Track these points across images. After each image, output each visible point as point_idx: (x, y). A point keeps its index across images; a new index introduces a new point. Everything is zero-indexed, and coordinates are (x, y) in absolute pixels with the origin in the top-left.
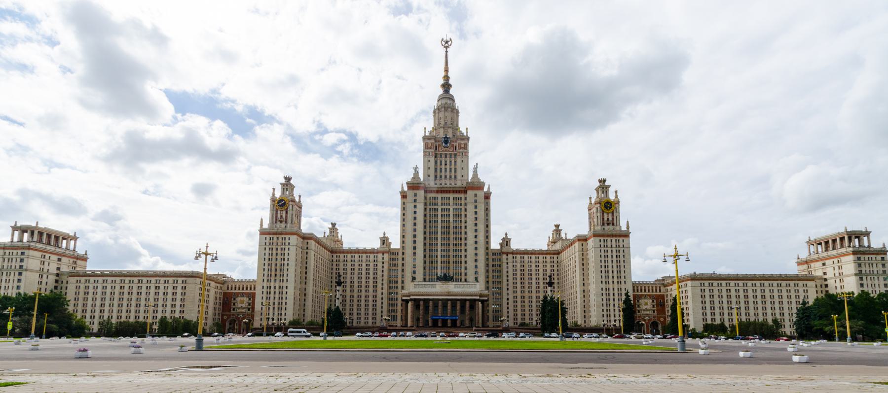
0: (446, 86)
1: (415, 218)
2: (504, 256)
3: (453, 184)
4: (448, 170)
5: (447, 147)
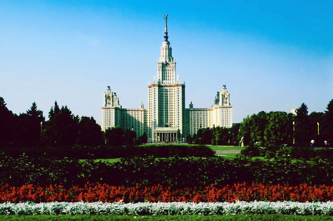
0: (166, 37)
2: (190, 112)
3: (169, 83)
4: (167, 76)
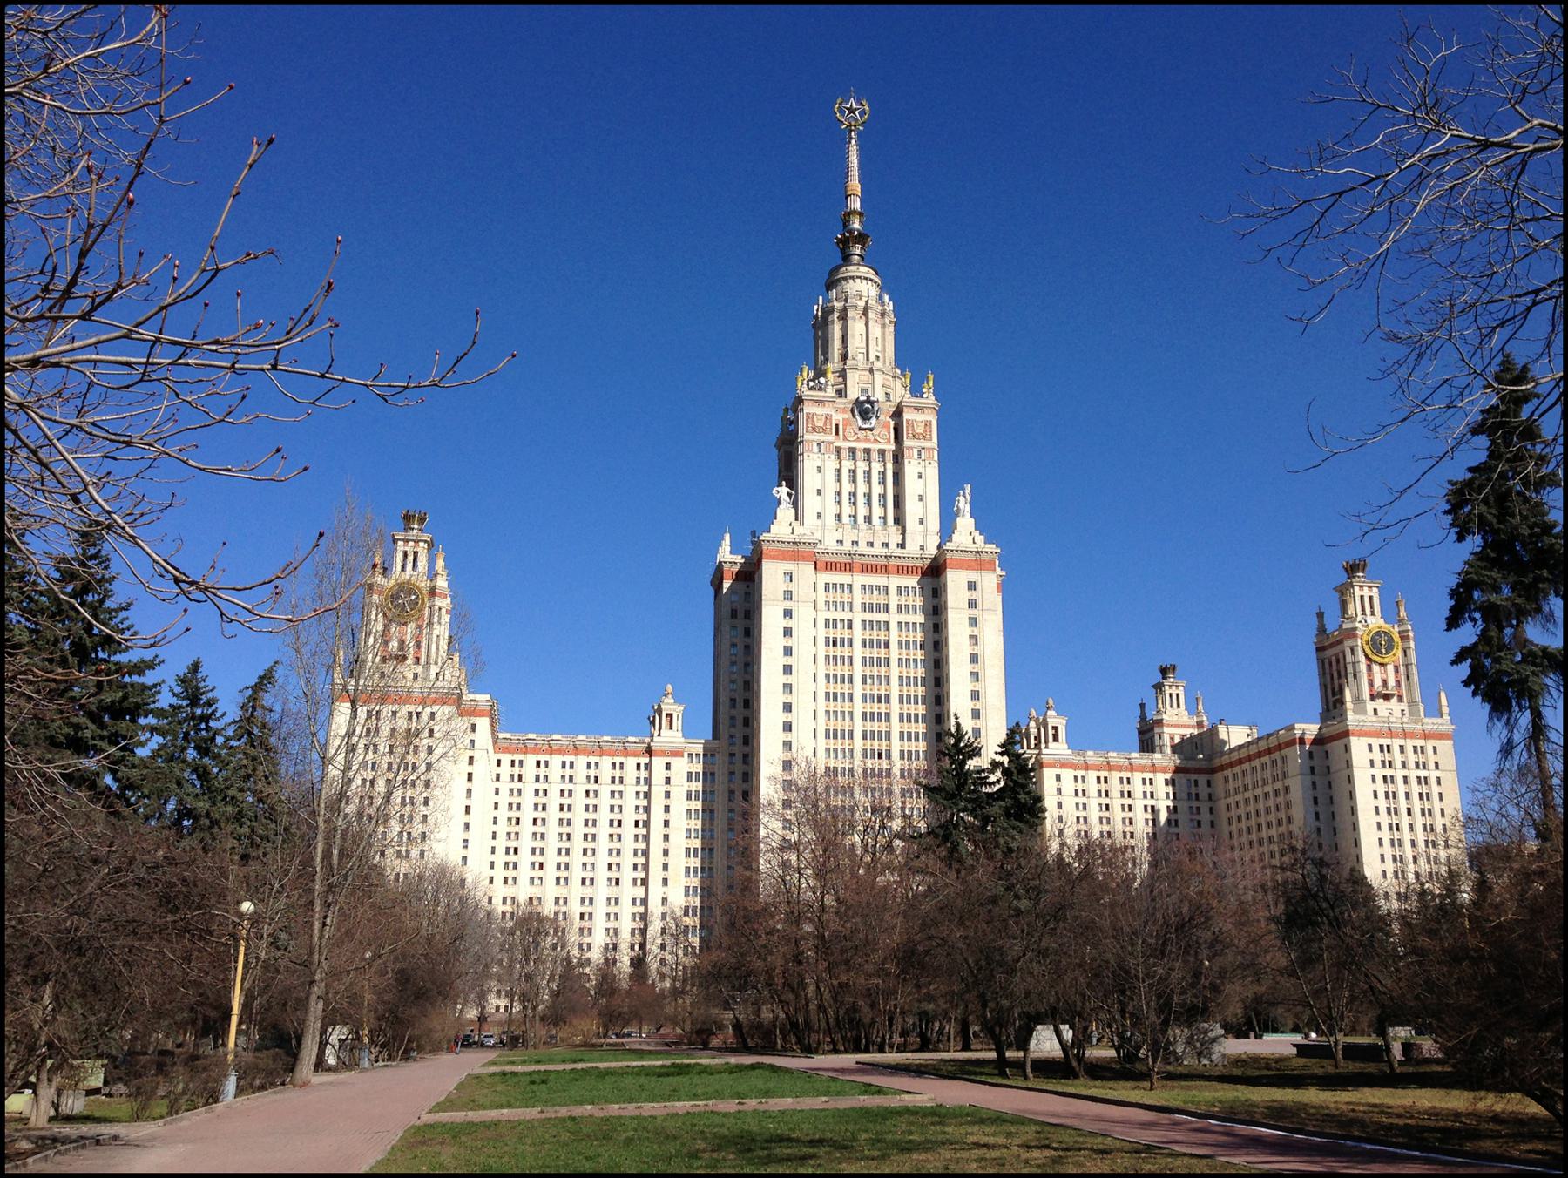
1: (788, 651)
5: (871, 430)
